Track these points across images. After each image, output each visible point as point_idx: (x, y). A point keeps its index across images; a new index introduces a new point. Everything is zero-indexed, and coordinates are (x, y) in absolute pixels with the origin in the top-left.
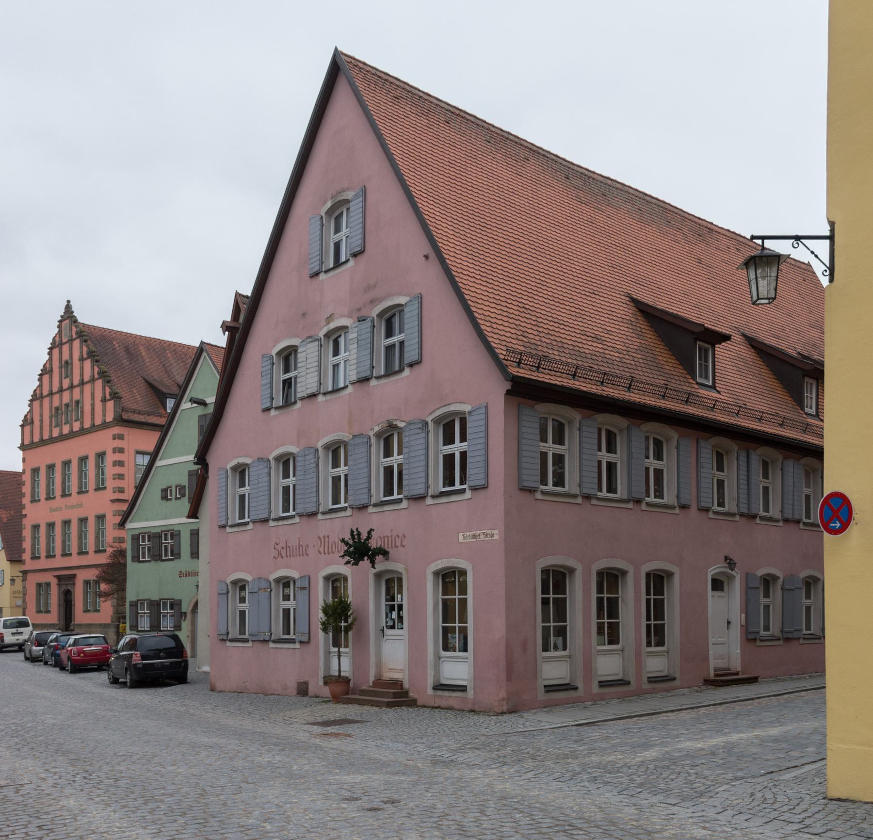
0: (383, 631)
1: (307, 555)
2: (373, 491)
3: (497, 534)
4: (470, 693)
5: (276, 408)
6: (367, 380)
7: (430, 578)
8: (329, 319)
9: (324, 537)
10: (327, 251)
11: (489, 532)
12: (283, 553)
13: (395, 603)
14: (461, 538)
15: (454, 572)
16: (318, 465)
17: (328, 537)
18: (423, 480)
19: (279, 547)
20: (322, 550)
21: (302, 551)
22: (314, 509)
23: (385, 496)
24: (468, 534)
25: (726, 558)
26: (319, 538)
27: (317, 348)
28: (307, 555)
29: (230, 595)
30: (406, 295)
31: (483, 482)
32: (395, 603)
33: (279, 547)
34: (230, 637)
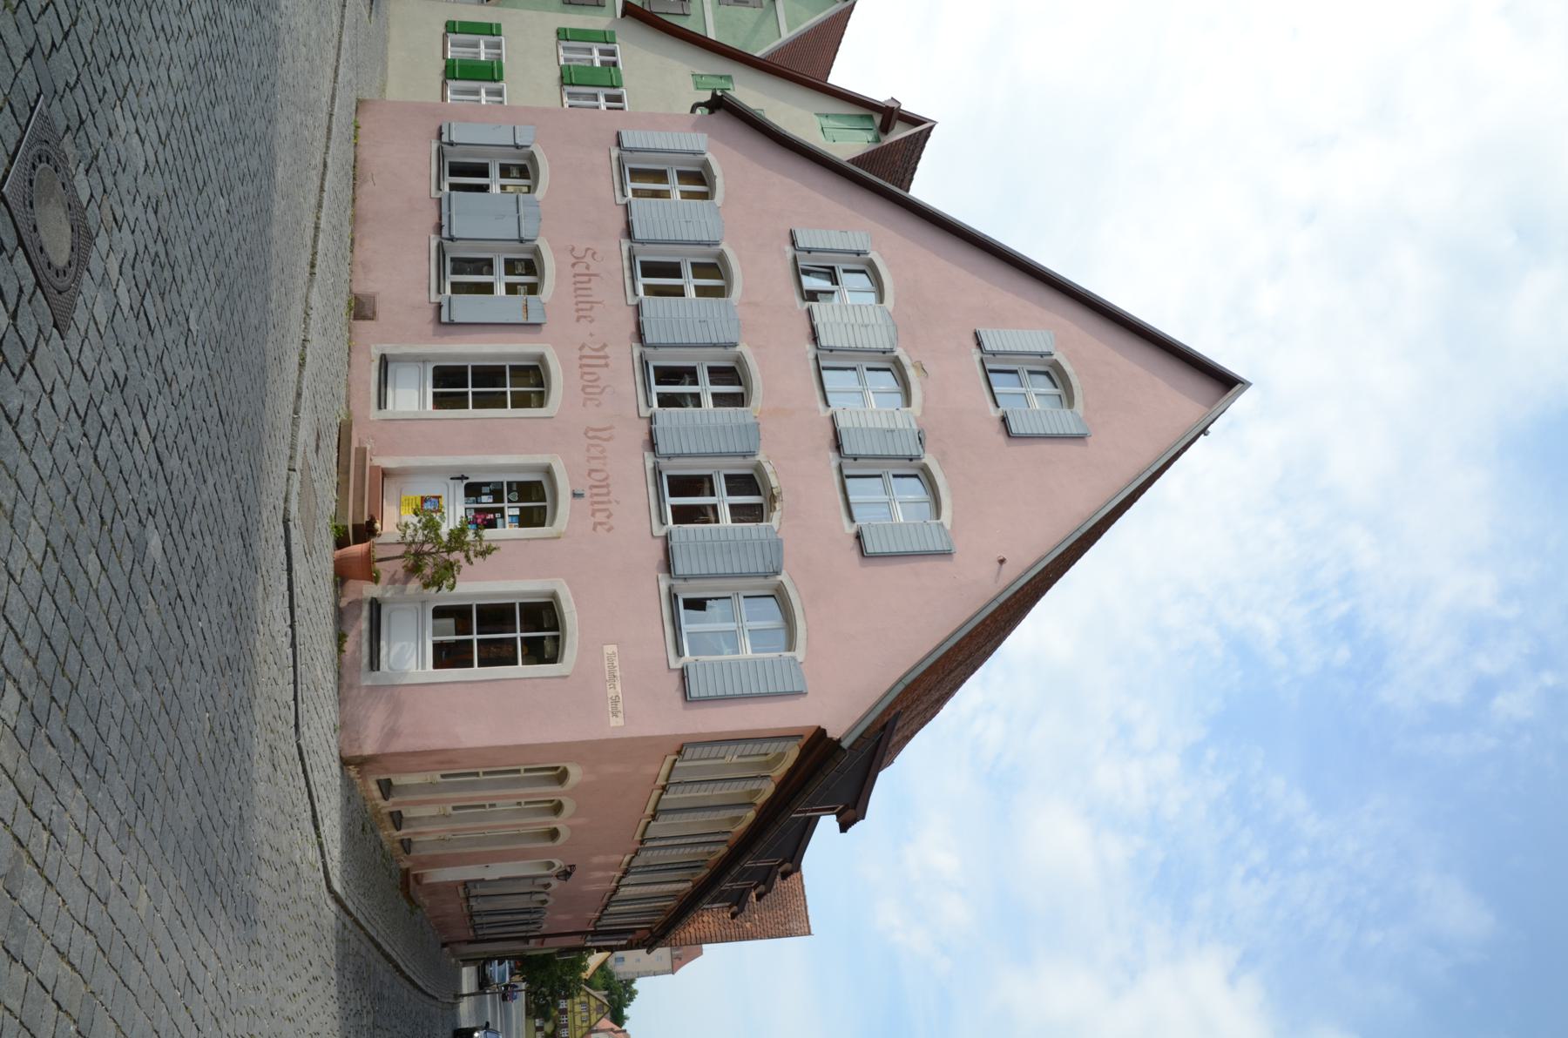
0: (462, 478)
1: (578, 320)
2: (676, 461)
3: (616, 722)
4: (367, 680)
5: (795, 258)
6: (838, 447)
7: (540, 459)
8: (922, 369)
9: (606, 357)
10: (1007, 361)
11: (620, 707)
12: (580, 269)
13: (506, 504)
14: (610, 649)
15: (557, 629)
16: (715, 345)
17: (606, 365)
18: (696, 571)
19: (588, 259)
20: (587, 352)
21: (583, 313)
22: (649, 340)
23: (656, 368)
24: (616, 663)
25: (572, 867)
26: (605, 346)
27: (881, 346)
28: (578, 320)
29: (517, 244)
30: (953, 521)
31: (694, 693)
32: (506, 504)
33: (588, 259)
34: (447, 244)
